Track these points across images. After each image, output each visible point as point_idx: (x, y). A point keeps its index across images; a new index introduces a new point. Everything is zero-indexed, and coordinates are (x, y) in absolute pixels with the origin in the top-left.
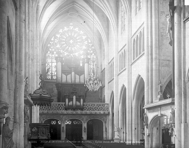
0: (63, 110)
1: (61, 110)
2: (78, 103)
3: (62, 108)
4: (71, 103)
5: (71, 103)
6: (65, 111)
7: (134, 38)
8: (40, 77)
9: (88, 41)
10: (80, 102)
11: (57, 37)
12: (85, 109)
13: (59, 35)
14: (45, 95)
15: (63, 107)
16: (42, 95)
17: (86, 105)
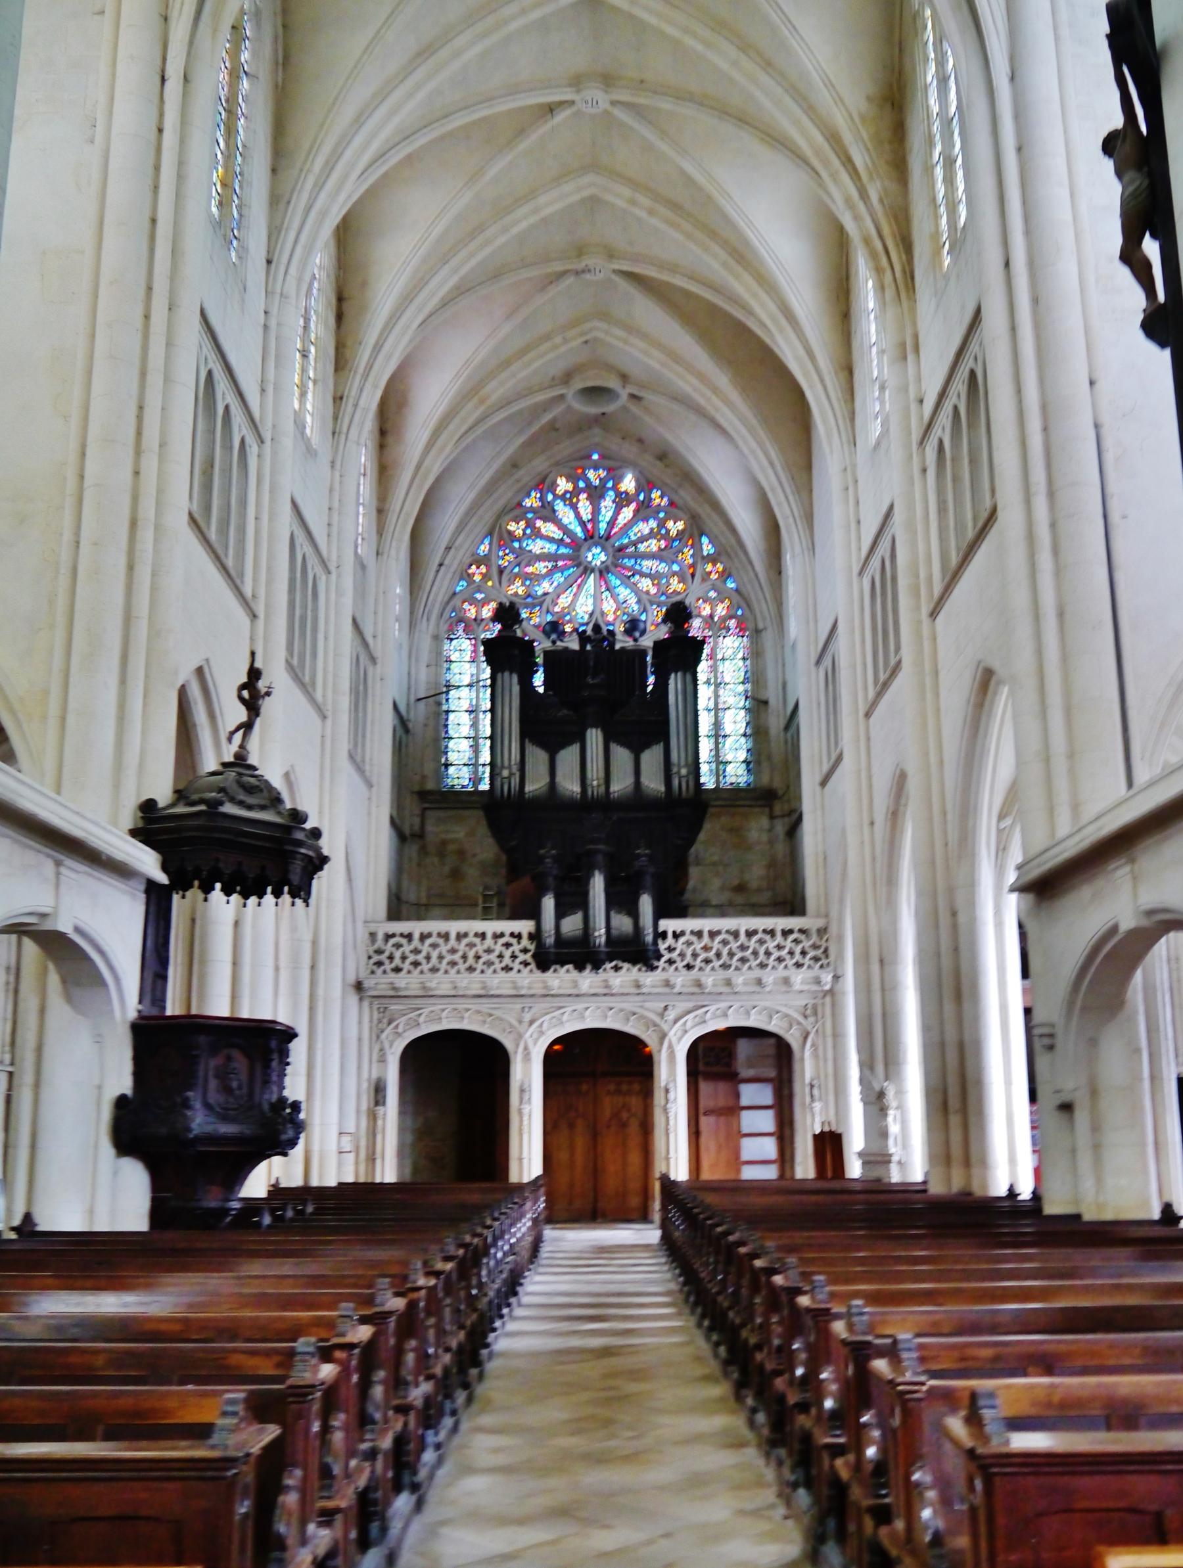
1: (507, 969)
2: (622, 923)
3: (514, 957)
4: (572, 925)
5: (572, 925)
6: (538, 974)
7: (937, 432)
8: (243, 687)
9: (697, 547)
10: (634, 914)
11: (510, 533)
12: (671, 962)
13: (522, 524)
14: (250, 808)
15: (525, 951)
16: (229, 808)
17: (676, 936)
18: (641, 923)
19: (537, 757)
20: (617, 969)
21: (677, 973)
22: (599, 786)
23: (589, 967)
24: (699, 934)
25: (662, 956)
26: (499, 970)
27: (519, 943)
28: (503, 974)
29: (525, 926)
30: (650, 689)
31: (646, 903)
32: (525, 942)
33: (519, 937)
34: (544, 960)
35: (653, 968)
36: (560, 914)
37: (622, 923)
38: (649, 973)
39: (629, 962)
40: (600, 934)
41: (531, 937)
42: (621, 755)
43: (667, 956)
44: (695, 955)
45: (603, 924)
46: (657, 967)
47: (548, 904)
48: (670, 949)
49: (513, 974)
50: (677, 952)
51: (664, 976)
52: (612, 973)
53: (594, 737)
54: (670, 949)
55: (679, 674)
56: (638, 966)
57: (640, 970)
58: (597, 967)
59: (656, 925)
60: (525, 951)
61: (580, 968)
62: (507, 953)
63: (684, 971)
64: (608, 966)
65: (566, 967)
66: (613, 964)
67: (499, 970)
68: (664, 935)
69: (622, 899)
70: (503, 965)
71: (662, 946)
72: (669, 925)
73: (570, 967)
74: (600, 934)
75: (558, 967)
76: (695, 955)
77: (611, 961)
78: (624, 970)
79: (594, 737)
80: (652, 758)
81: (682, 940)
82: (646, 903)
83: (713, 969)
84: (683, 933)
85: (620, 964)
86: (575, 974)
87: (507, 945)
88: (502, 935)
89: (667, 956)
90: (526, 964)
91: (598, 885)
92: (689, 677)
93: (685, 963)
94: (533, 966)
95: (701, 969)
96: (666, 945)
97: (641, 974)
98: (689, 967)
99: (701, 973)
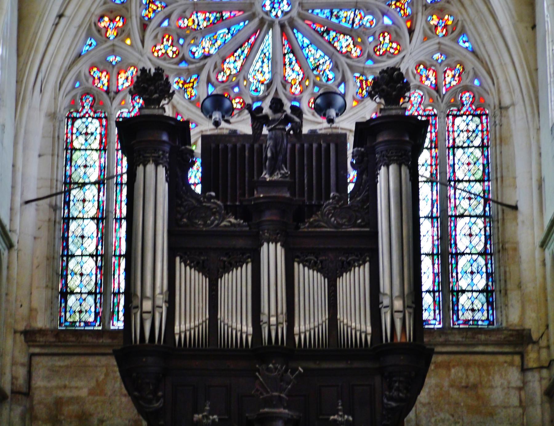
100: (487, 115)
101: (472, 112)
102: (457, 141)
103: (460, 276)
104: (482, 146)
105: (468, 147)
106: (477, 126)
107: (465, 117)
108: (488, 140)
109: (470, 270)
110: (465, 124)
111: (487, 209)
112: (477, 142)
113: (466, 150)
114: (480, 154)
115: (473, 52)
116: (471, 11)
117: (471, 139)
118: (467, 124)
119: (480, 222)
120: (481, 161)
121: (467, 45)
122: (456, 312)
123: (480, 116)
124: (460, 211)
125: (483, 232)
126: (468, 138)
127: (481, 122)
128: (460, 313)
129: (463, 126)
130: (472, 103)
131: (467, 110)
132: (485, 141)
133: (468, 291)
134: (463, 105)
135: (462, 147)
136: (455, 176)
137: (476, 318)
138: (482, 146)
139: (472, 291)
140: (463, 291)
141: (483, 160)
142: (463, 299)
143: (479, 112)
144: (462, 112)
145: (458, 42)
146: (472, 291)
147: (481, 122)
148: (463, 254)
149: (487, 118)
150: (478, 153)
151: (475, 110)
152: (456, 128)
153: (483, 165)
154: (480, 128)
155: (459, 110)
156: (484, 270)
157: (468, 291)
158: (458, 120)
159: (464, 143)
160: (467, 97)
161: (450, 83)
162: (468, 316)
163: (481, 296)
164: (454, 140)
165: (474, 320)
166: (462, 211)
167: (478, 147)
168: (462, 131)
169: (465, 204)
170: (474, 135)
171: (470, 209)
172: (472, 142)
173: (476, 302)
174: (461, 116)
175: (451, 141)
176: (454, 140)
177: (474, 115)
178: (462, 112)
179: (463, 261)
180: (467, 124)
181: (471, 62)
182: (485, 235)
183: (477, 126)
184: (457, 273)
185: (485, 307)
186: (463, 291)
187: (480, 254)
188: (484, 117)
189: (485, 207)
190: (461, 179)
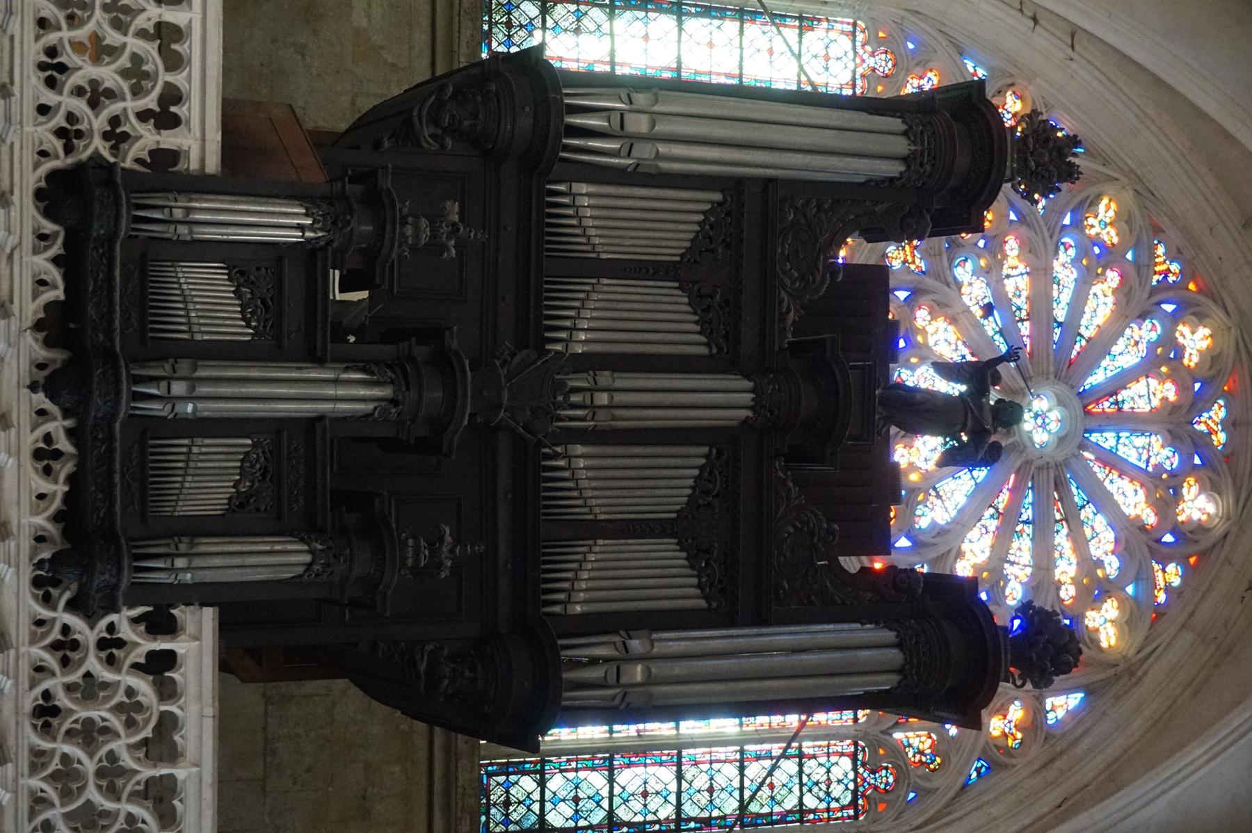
0: (43, 133)
1: (53, 69)
2: (207, 479)
3: (96, 95)
4: (207, 300)
5: (207, 300)
6: (29, 178)
12: (66, 647)
15: (116, 136)
18: (207, 545)
19: (669, 226)
20: (45, 456)
21: (25, 670)
22: (593, 408)
23: (58, 356)
24: (162, 743)
25: (91, 619)
26: (52, 38)
27: (143, 116)
28: (33, 51)
29: (199, 141)
30: (851, 564)
31: (277, 559)
32: (148, 138)
33: (165, 119)
34: (80, 197)
35: (44, 585)
36: (243, 262)
37: (207, 479)
38: (27, 573)
39: (67, 498)
40: (184, 396)
41: (164, 159)
42: (671, 481)
43: (87, 634)
44: (89, 734)
45: (210, 409)
46: (47, 600)
47: (283, 223)
48: (110, 645)
49: (30, 87)
50: (105, 675)
51: (19, 629)
52: (31, 440)
53: (727, 399)
54: (110, 645)
55: (895, 656)
56: (52, 529)
57: (40, 539)
58: (50, 382)
59: (200, 595)
60: (116, 136)
61: (56, 325)
62: (108, 74)
63: (30, 700)
64: (57, 427)
65: (55, 275)
66: (64, 444)
67: (52, 38)
68: (160, 624)
69: (296, 475)
70: (68, 57)
71: (123, 621)
72: (197, 641)
73: (59, 294)
74: (184, 396)
75: (56, 249)
76: (89, 734)
77: (70, 433)
78: (45, 486)
79: (727, 399)
80: (660, 572)
81: (143, 686)
82: (277, 559)
83: (39, 801)
84: (167, 691)
85: (65, 469)
86: (29, 308)
87: (137, 74)
88: (174, 62)
89: (87, 634)
90: (69, 135)
91: (342, 393)
92: (886, 683)
93: (62, 700)
94: (61, 162)
95: (38, 759)
96: (126, 632)
97: (26, 543)
98: (46, 712)
99: (24, 760)
100: (856, 817)
101: (861, 789)
102: (813, 762)
103: (571, 775)
104: (801, 810)
105: (801, 785)
106: (837, 800)
107: (851, 775)
108: (814, 821)
109: (581, 795)
110: (841, 777)
111: (692, 825)
112: (810, 802)
113: (797, 780)
114: (788, 807)
115: (965, 786)
116: (1036, 782)
117: (816, 789)
118: (839, 781)
119: (667, 812)
120: (777, 809)
121: (974, 775)
122: (505, 770)
123: (854, 804)
124: (689, 771)
125: (650, 817)
126: (817, 784)
127: (842, 808)
128: (502, 779)
129: (837, 773)
130: (876, 788)
131: (864, 780)
132: (811, 816)
133: (542, 793)
134: (873, 772)
135: (801, 772)
136: (750, 760)
137: (493, 811)
138: (801, 810)
139: (542, 801)
140: (542, 784)
141: (778, 814)
142: (528, 783)
143: (860, 802)
144: (861, 770)
145: (979, 759)
146: (542, 801)
147: (842, 808)
148: (611, 781)
149: (849, 817)
150: (790, 803)
151: (863, 795)
152: (834, 759)
153: (771, 814)
154: (834, 805)
155: (863, 765)
156: (582, 823)
157: (542, 793)
158: (846, 763)
159: (808, 776)
160: (886, 778)
161: (910, 745)
162: (497, 795)
163: (533, 818)
164: (814, 757)
165: (488, 806)
166: (688, 776)
167: (801, 803)
168: (828, 771)
169: (702, 782)
170: (822, 795)
171: (691, 791)
172: (810, 791)
173: (522, 810)
174: (855, 769)
175: (811, 751)
176: (814, 757)
177: (855, 792)
178: (861, 770)
179: (597, 780)
180: (839, 781)
181: (946, 785)
182: (645, 823)
183: (837, 800)
184: (576, 770)
185: (512, 828)
186: (542, 784)
187: (611, 813)
188: (851, 812)
189: (695, 820)
190: (746, 772)
